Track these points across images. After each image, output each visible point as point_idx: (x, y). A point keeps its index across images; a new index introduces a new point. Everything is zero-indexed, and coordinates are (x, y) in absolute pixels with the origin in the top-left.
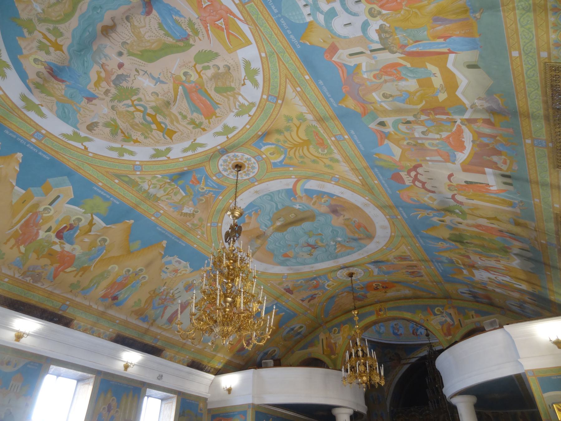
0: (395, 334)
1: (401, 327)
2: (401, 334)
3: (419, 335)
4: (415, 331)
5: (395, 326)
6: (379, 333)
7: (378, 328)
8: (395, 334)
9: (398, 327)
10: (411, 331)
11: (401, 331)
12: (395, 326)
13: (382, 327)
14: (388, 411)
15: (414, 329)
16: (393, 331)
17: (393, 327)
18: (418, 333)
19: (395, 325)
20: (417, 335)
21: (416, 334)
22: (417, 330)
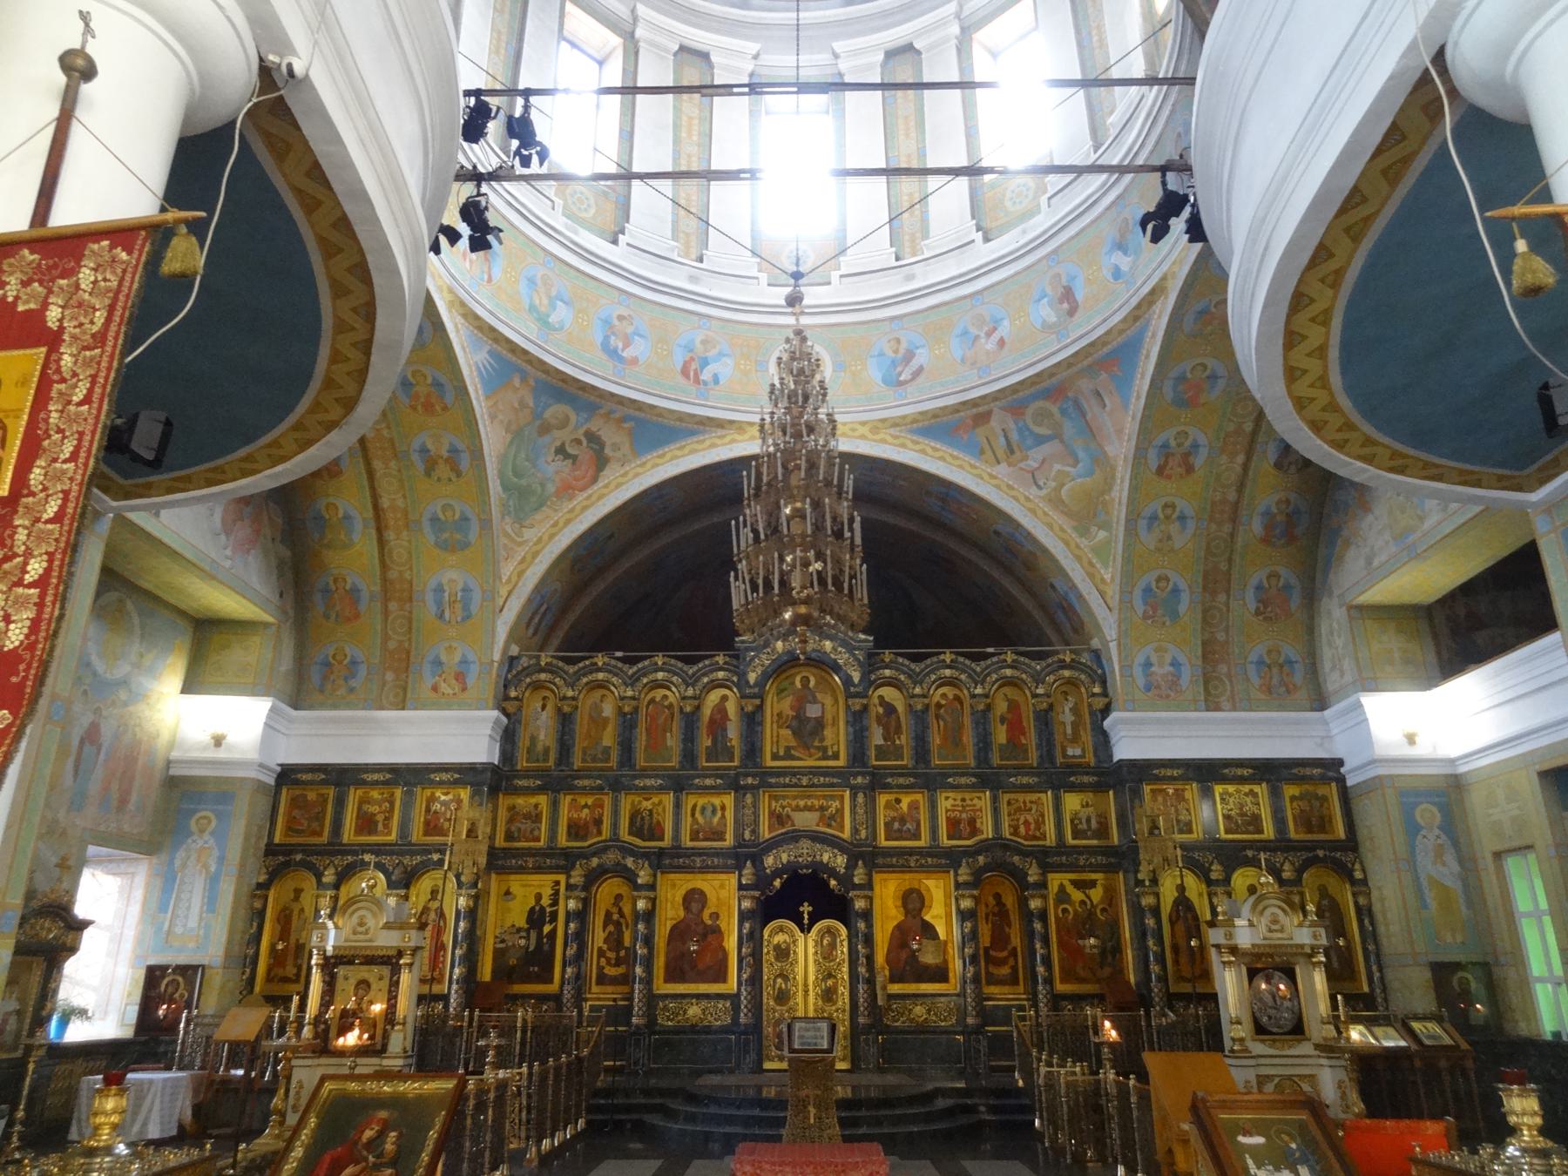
0: (613, 353)
1: (641, 336)
2: (634, 361)
3: (705, 383)
4: (694, 366)
5: (616, 322)
6: (543, 321)
7: (545, 301)
8: (613, 353)
9: (630, 330)
10: (679, 360)
11: (638, 349)
12: (616, 322)
13: (559, 303)
14: (497, 656)
15: (692, 359)
16: (606, 338)
17: (607, 322)
18: (706, 375)
19: (621, 318)
20: (697, 381)
21: (696, 375)
22: (705, 362)
